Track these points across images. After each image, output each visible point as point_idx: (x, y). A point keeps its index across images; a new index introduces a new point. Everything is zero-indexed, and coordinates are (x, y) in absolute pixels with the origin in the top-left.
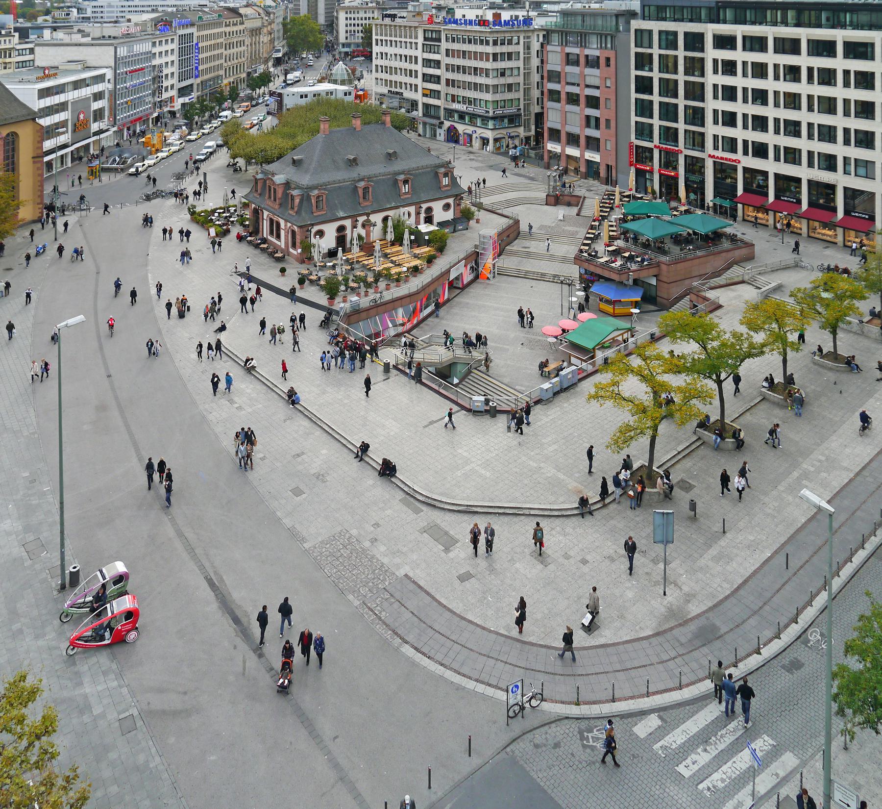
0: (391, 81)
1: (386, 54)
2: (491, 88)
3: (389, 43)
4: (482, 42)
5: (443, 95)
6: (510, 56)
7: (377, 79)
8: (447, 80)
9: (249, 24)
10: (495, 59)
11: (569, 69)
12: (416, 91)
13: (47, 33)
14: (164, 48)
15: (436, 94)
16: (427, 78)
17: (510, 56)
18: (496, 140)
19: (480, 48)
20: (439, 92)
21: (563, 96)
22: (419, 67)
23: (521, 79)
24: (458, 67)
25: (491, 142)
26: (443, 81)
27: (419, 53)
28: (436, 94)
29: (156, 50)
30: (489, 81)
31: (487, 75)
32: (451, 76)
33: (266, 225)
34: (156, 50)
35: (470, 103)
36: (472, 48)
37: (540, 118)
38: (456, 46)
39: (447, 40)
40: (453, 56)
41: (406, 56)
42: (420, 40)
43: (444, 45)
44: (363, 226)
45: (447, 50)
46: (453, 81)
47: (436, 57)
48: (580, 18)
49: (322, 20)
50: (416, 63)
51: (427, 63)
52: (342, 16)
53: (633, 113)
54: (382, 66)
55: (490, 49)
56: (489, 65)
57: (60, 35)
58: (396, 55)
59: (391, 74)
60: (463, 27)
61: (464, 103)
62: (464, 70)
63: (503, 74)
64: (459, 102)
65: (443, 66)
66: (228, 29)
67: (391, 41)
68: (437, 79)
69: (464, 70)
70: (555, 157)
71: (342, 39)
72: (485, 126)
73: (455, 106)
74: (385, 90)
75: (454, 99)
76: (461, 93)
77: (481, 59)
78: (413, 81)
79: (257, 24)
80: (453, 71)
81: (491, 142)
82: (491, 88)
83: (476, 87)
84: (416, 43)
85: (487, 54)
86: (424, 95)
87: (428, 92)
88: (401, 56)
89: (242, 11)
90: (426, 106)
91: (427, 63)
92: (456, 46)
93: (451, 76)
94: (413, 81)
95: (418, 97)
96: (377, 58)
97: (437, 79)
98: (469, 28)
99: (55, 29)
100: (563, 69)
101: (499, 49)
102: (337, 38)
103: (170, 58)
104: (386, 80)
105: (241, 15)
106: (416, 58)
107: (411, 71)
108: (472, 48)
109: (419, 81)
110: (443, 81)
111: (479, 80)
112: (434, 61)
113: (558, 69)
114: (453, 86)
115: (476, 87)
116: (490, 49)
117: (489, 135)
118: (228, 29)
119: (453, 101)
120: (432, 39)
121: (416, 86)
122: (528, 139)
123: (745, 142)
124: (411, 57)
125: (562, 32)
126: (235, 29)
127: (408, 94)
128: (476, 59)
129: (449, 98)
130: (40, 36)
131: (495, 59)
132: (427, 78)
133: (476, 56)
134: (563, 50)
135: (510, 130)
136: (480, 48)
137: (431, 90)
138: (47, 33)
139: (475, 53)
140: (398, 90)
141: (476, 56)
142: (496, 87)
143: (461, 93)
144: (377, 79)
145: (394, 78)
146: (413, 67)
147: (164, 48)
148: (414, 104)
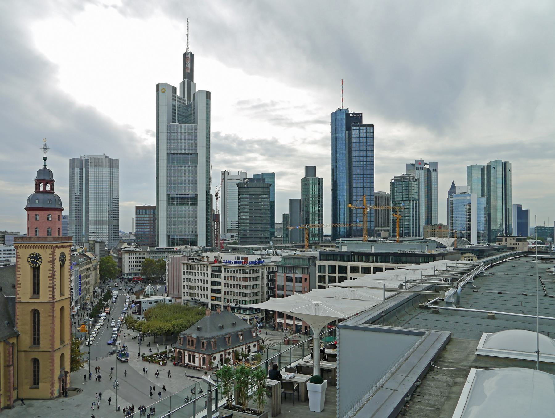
0: (193, 293)
1: (190, 279)
2: (248, 295)
3: (206, 274)
4: (243, 273)
5: (222, 299)
6: (255, 278)
7: (184, 293)
8: (225, 292)
10: (250, 281)
11: (288, 284)
12: (207, 298)
15: (219, 299)
16: (213, 291)
17: (255, 278)
18: (251, 320)
19: (242, 275)
20: (220, 298)
22: (209, 286)
23: (260, 290)
24: (231, 285)
25: (248, 321)
26: (223, 292)
27: (209, 278)
28: (219, 299)
30: (247, 291)
31: (246, 288)
32: (227, 289)
35: (237, 302)
36: (238, 275)
38: (229, 274)
39: (225, 271)
40: (228, 280)
41: (201, 280)
42: (210, 272)
43: (223, 274)
45: (225, 277)
46: (228, 292)
47: (219, 280)
48: (292, 261)
50: (207, 283)
51: (213, 283)
54: (187, 286)
55: (247, 276)
56: (247, 283)
58: (195, 280)
59: (193, 289)
60: (233, 265)
61: (234, 303)
62: (234, 286)
63: (253, 288)
64: (231, 302)
65: (223, 285)
67: (195, 273)
68: (219, 291)
69: (234, 286)
70: (280, 324)
72: (244, 313)
74: (189, 298)
75: (228, 301)
76: (232, 297)
77: (243, 281)
78: (206, 293)
80: (228, 287)
81: (248, 321)
82: (248, 295)
83: (240, 294)
84: (207, 273)
85: (246, 278)
86: (212, 300)
87: (214, 298)
88: (198, 280)
90: (213, 305)
91: (213, 283)
92: (229, 274)
93: (227, 289)
94: (206, 293)
95: (209, 301)
96: (184, 282)
97: (219, 291)
98: (236, 265)
100: (285, 284)
101: (252, 275)
104: (190, 293)
106: (207, 281)
107: (204, 288)
108: (238, 275)
110: (223, 292)
111: (244, 291)
112: (218, 282)
113: (283, 284)
114: (228, 294)
115: (240, 294)
116: (247, 276)
117: (247, 317)
119: (228, 302)
120: (216, 271)
121: (207, 295)
122: (262, 318)
124: (204, 280)
125: (284, 267)
127: (202, 300)
128: (240, 280)
129: (226, 300)
131: (250, 281)
132: (213, 291)
133: (240, 279)
134: (285, 275)
135: (256, 315)
136: (242, 275)
137: (216, 297)
139: (240, 277)
140: (197, 298)
141: (240, 279)
142: (250, 293)
143: (232, 297)
144: (184, 293)
145: (194, 291)
146: (206, 286)
148: (207, 304)
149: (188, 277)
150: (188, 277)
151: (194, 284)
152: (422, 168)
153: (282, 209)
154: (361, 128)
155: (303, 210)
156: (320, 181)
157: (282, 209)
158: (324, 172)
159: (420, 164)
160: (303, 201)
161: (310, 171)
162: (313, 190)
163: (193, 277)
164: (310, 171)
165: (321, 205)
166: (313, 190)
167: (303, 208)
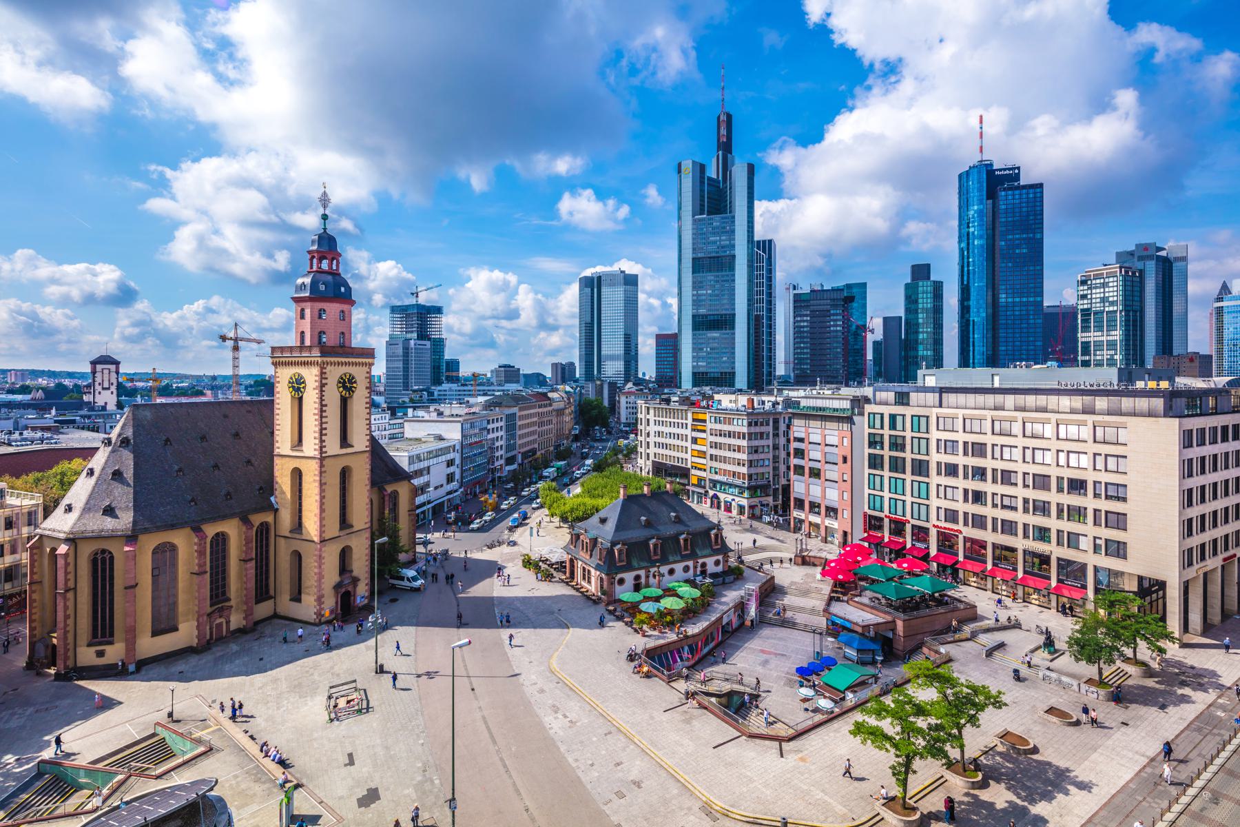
9: (555, 406)
13: (410, 411)
14: (496, 425)
21: (807, 471)
22: (688, 444)
27: (688, 432)
29: (490, 427)
32: (714, 452)
33: (579, 573)
34: (490, 427)
37: (787, 489)
44: (654, 576)
49: (606, 403)
52: (623, 400)
53: (866, 486)
57: (421, 413)
63: (756, 452)
66: (540, 410)
71: (623, 420)
73: (717, 477)
79: (562, 405)
89: (550, 395)
99: (414, 408)
102: (619, 418)
103: (500, 434)
105: (549, 399)
109: (688, 456)
118: (540, 410)
123: (966, 514)
126: (545, 410)
130: (406, 414)
138: (410, 411)
146: (684, 444)
147: (496, 425)
149: (661, 429)
150: (661, 429)
151: (668, 441)
152: (1150, 257)
153: (876, 331)
154: (1017, 192)
155: (906, 334)
156: (938, 289)
157: (876, 331)
158: (948, 276)
159: (1146, 249)
160: (906, 323)
161: (921, 272)
162: (925, 302)
163: (667, 430)
164: (921, 272)
165: (938, 326)
166: (925, 302)
167: (906, 330)
